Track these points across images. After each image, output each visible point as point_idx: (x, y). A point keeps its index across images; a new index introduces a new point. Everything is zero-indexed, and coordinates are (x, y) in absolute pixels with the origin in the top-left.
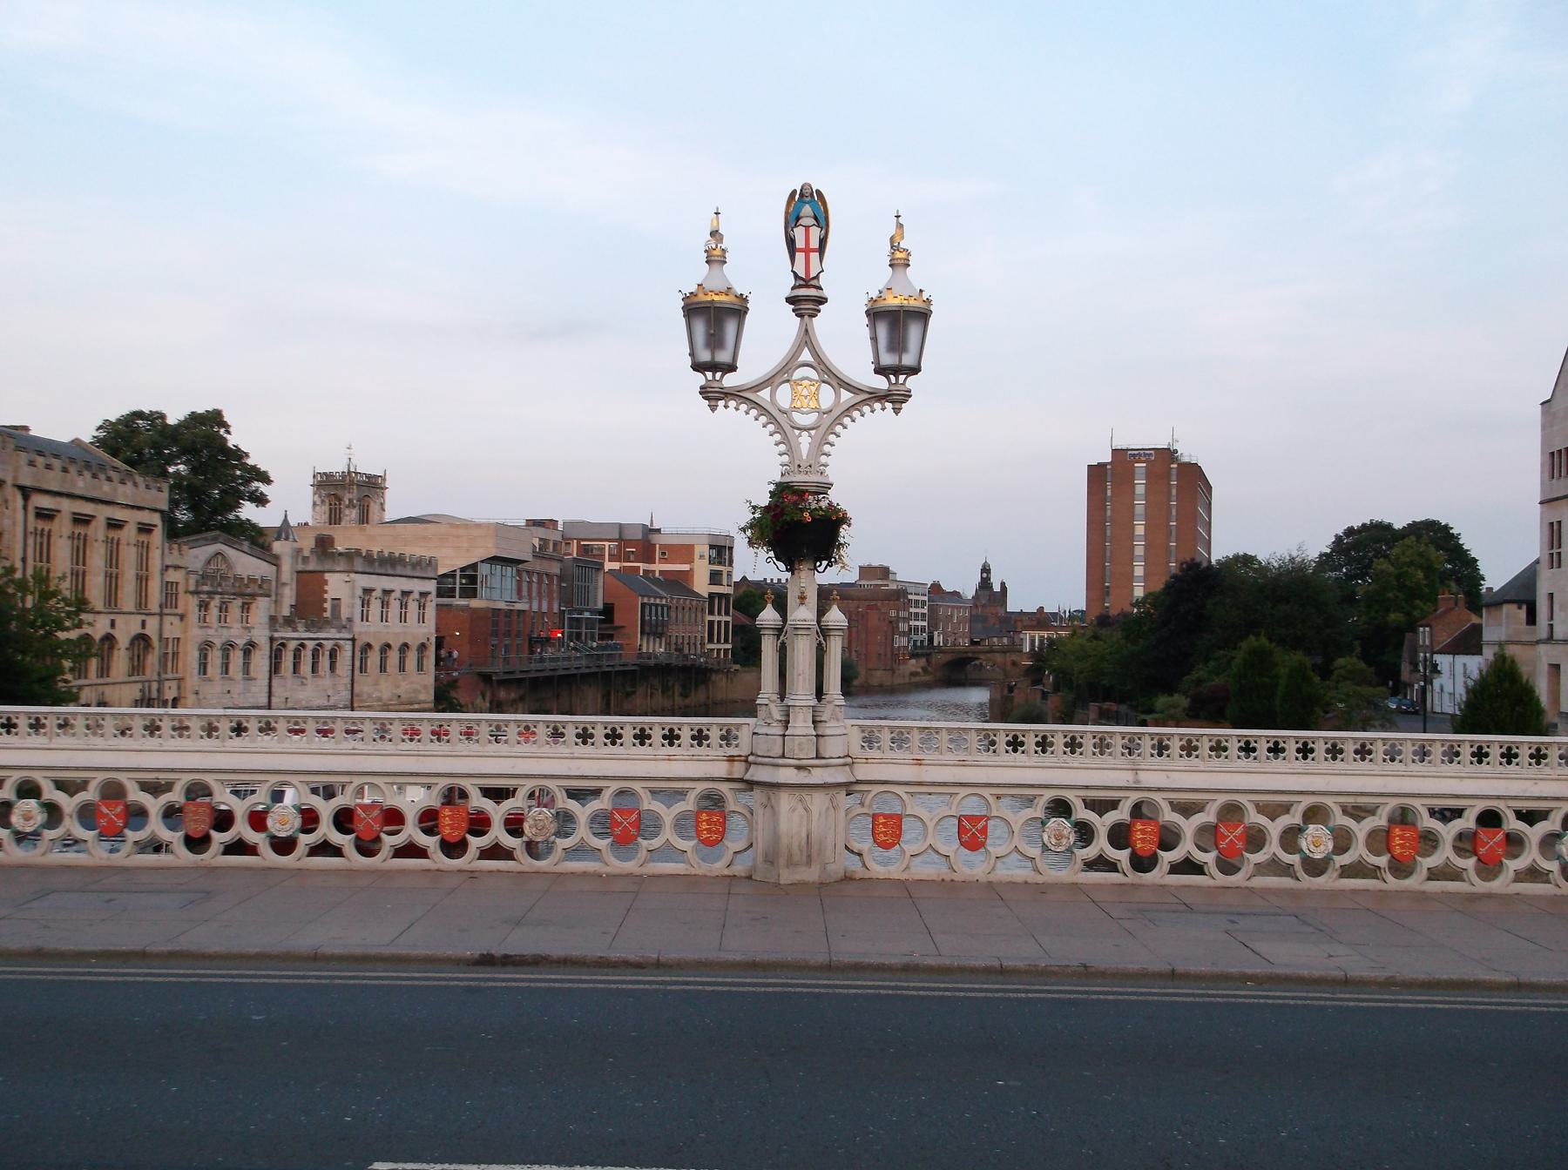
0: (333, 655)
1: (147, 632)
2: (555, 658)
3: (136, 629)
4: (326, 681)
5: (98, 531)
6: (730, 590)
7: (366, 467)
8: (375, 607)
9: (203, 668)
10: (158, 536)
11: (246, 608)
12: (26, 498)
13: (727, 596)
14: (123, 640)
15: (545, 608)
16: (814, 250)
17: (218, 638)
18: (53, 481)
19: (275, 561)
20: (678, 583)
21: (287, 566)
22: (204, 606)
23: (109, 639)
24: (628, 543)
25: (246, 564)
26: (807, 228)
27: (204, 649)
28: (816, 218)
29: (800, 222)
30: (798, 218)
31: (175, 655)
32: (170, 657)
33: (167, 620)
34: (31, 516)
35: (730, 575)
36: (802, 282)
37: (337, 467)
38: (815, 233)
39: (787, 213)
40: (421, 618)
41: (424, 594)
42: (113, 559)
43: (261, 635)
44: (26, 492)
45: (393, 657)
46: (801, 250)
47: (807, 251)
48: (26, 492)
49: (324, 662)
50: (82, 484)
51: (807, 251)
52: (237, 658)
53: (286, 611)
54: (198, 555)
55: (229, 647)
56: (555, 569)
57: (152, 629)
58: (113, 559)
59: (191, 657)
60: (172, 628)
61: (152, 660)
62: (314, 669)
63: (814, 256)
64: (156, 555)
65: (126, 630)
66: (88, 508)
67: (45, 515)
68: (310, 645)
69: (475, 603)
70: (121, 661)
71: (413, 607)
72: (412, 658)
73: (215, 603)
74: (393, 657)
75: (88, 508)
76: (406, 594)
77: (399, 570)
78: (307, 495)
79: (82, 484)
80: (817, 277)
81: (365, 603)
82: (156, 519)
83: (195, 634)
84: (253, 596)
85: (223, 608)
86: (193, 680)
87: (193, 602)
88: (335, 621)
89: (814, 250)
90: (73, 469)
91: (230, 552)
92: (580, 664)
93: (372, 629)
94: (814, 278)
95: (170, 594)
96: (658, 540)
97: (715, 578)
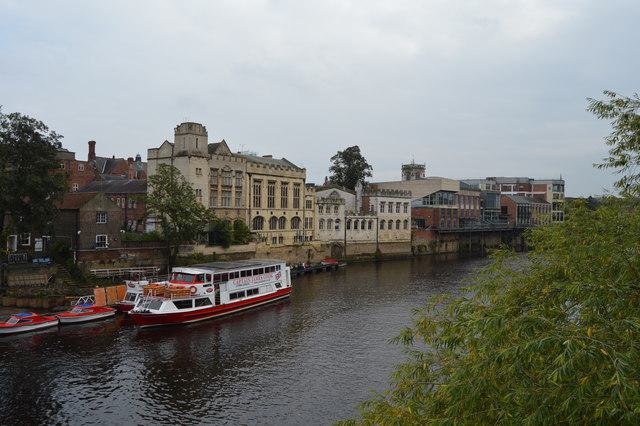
0: (370, 223)
2: (477, 225)
4: (367, 231)
5: (278, 186)
7: (418, 162)
8: (386, 208)
11: (336, 208)
15: (472, 208)
17: (326, 217)
18: (260, 170)
19: (355, 193)
20: (542, 199)
23: (283, 219)
24: (521, 184)
27: (322, 221)
31: (311, 223)
32: (309, 223)
33: (306, 213)
34: (252, 181)
35: (562, 195)
37: (409, 163)
40: (405, 211)
42: (284, 192)
43: (342, 216)
44: (250, 175)
45: (394, 225)
48: (250, 175)
49: (367, 225)
52: (334, 224)
53: (358, 209)
55: (330, 221)
56: (477, 194)
57: (300, 215)
59: (317, 224)
60: (309, 214)
61: (301, 224)
62: (363, 228)
64: (301, 193)
65: (290, 215)
66: (274, 179)
67: (259, 181)
68: (361, 220)
69: (434, 206)
70: (288, 225)
71: (402, 208)
72: (402, 225)
73: (325, 207)
74: (394, 225)
75: (274, 179)
79: (270, 172)
83: (318, 216)
85: (328, 209)
86: (317, 230)
88: (373, 213)
90: (267, 167)
92: (487, 227)
93: (386, 215)
95: (309, 204)
96: (532, 183)
97: (556, 197)
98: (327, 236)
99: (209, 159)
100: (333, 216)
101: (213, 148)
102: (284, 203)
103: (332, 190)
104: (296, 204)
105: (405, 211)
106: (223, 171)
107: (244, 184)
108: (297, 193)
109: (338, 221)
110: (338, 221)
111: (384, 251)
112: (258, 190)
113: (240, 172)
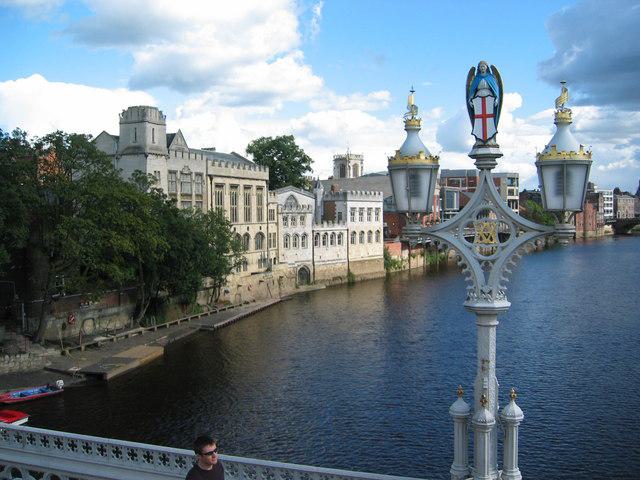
1: (262, 231)
3: (258, 230)
4: (338, 247)
5: (241, 191)
6: (517, 198)
9: (286, 245)
10: (265, 189)
11: (302, 219)
12: (211, 180)
13: (515, 200)
14: (252, 236)
16: (489, 116)
17: (291, 230)
21: (319, 200)
22: (285, 219)
23: (247, 235)
25: (305, 200)
26: (483, 98)
28: (491, 90)
29: (479, 93)
30: (477, 90)
32: (273, 241)
34: (213, 186)
36: (481, 143)
37: (343, 153)
38: (490, 103)
39: (468, 86)
40: (377, 219)
41: (377, 209)
43: (308, 229)
44: (211, 177)
45: (366, 236)
46: (478, 117)
47: (484, 117)
48: (211, 177)
50: (233, 171)
51: (484, 117)
54: (282, 196)
57: (264, 230)
58: (247, 201)
60: (273, 229)
61: (265, 241)
63: (490, 121)
68: (330, 233)
71: (373, 214)
72: (374, 236)
74: (366, 236)
76: (370, 209)
77: (370, 198)
78: (331, 165)
80: (494, 136)
81: (353, 214)
82: (264, 184)
83: (283, 230)
84: (305, 213)
85: (293, 219)
86: (282, 250)
87: (280, 217)
89: (489, 116)
90: (230, 166)
91: (296, 195)
94: (490, 139)
95: (271, 216)
98: (293, 258)
99: (168, 157)
100: (299, 230)
101: (171, 138)
102: (248, 217)
103: (288, 194)
104: (260, 218)
105: (377, 219)
106: (182, 173)
107: (205, 190)
108: (260, 202)
109: (305, 236)
110: (305, 236)
111: (356, 272)
112: (220, 200)
113: (199, 175)
